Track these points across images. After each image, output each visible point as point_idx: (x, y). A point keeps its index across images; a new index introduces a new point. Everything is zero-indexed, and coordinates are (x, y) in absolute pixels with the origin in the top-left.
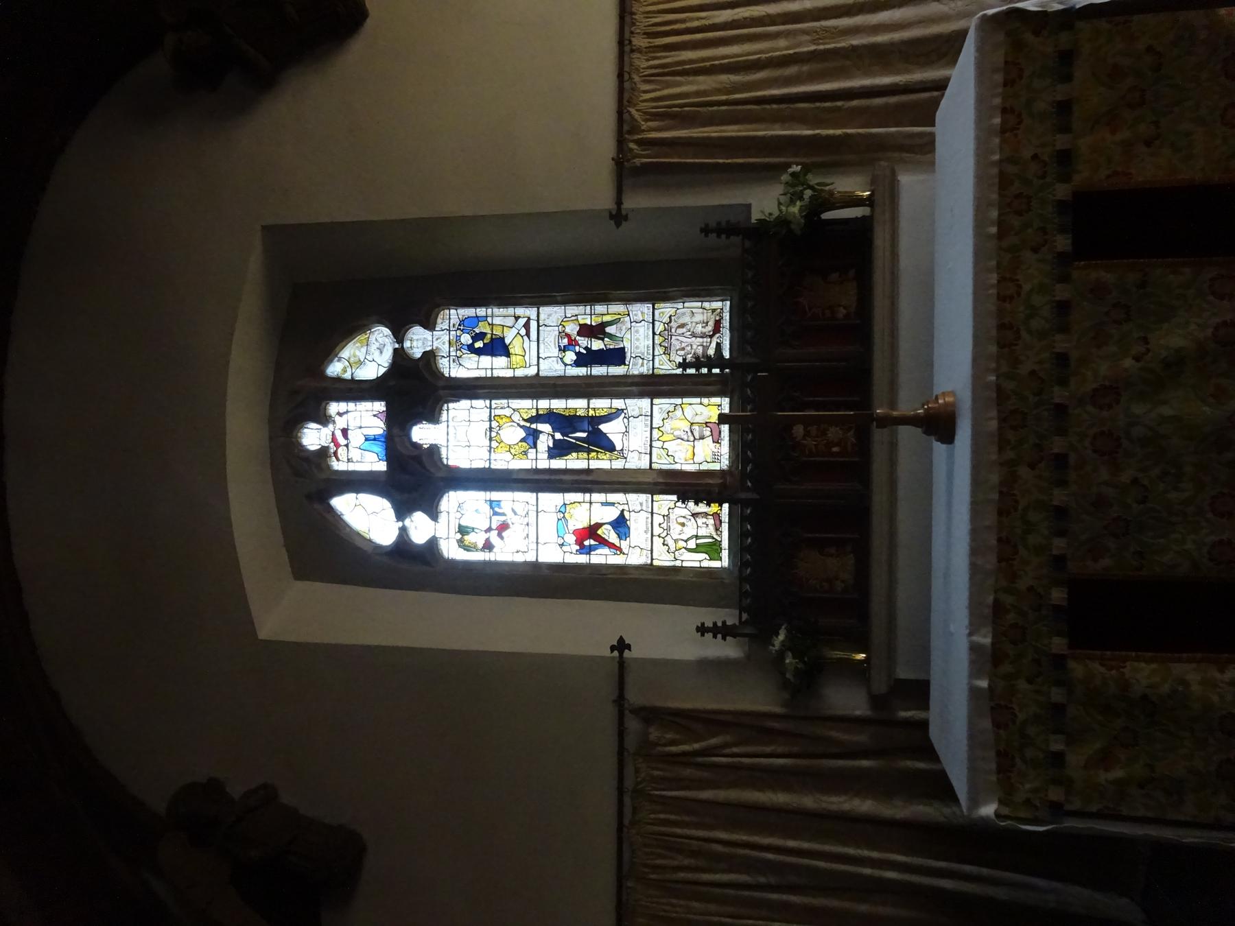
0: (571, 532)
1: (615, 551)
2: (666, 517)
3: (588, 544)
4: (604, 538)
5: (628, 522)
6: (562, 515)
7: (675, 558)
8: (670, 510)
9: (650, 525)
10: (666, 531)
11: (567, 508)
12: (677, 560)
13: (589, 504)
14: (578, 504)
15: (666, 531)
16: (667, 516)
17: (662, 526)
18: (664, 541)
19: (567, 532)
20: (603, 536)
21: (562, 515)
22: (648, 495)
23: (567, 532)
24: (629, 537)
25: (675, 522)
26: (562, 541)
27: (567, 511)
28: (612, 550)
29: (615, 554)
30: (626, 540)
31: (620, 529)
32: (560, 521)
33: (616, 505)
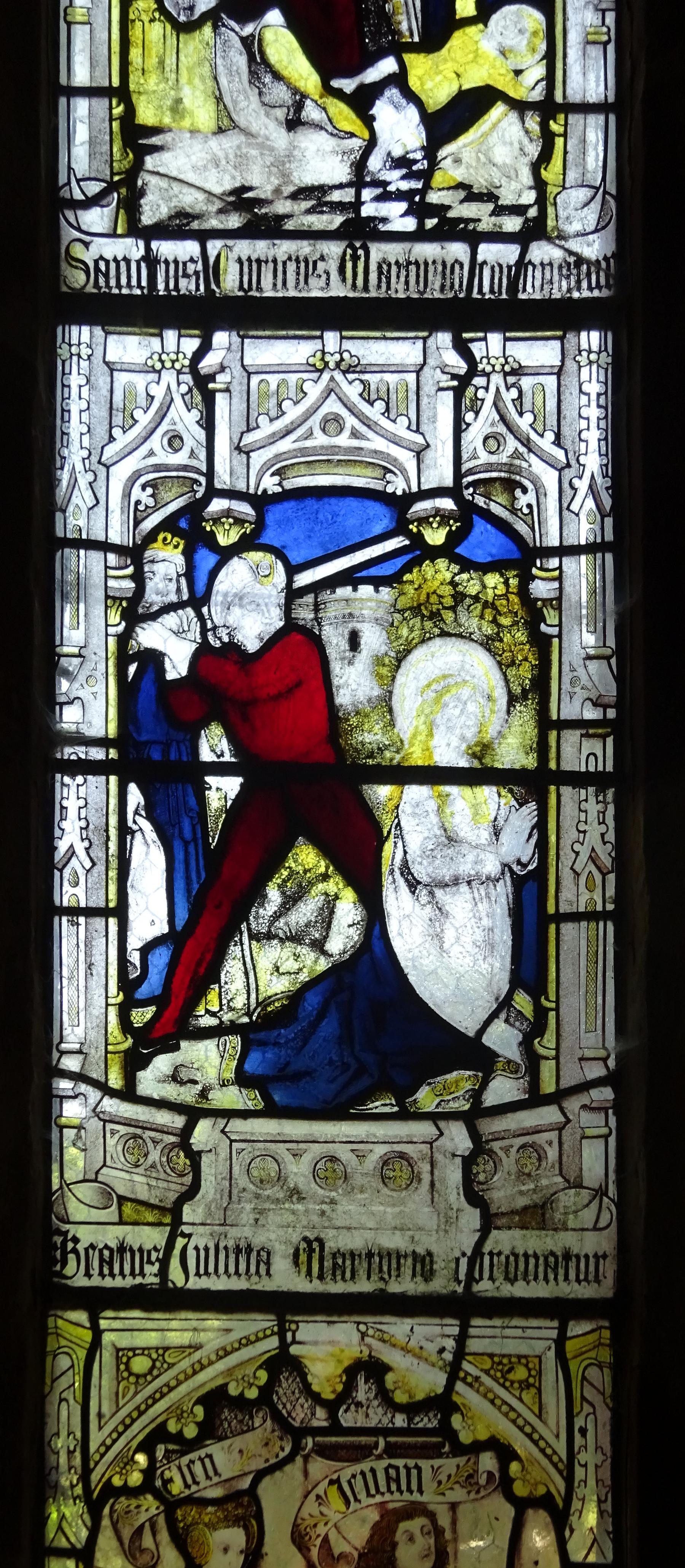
0: (304, 614)
1: (153, 984)
2: (426, 1421)
3: (206, 755)
4: (258, 895)
5: (382, 1105)
6: (436, 537)
7: (110, 1491)
8: (488, 1462)
9: (364, 1286)
10: (321, 1418)
11: (493, 579)
12: (94, 1508)
13: (530, 762)
14: (525, 672)
15: (321, 1418)
16: (446, 1431)
17: (363, 1391)
18: (241, 1403)
19: (304, 579)
20: (274, 895)
21: (436, 537)
22: (609, 1269)
23: (304, 579)
24: (271, 1111)
25: (396, 1500)
26: (226, 537)
27: (471, 584)
28: (160, 959)
29: (127, 985)
30: (242, 1079)
31: (329, 1027)
32: (382, 520)
33: (523, 1002)
